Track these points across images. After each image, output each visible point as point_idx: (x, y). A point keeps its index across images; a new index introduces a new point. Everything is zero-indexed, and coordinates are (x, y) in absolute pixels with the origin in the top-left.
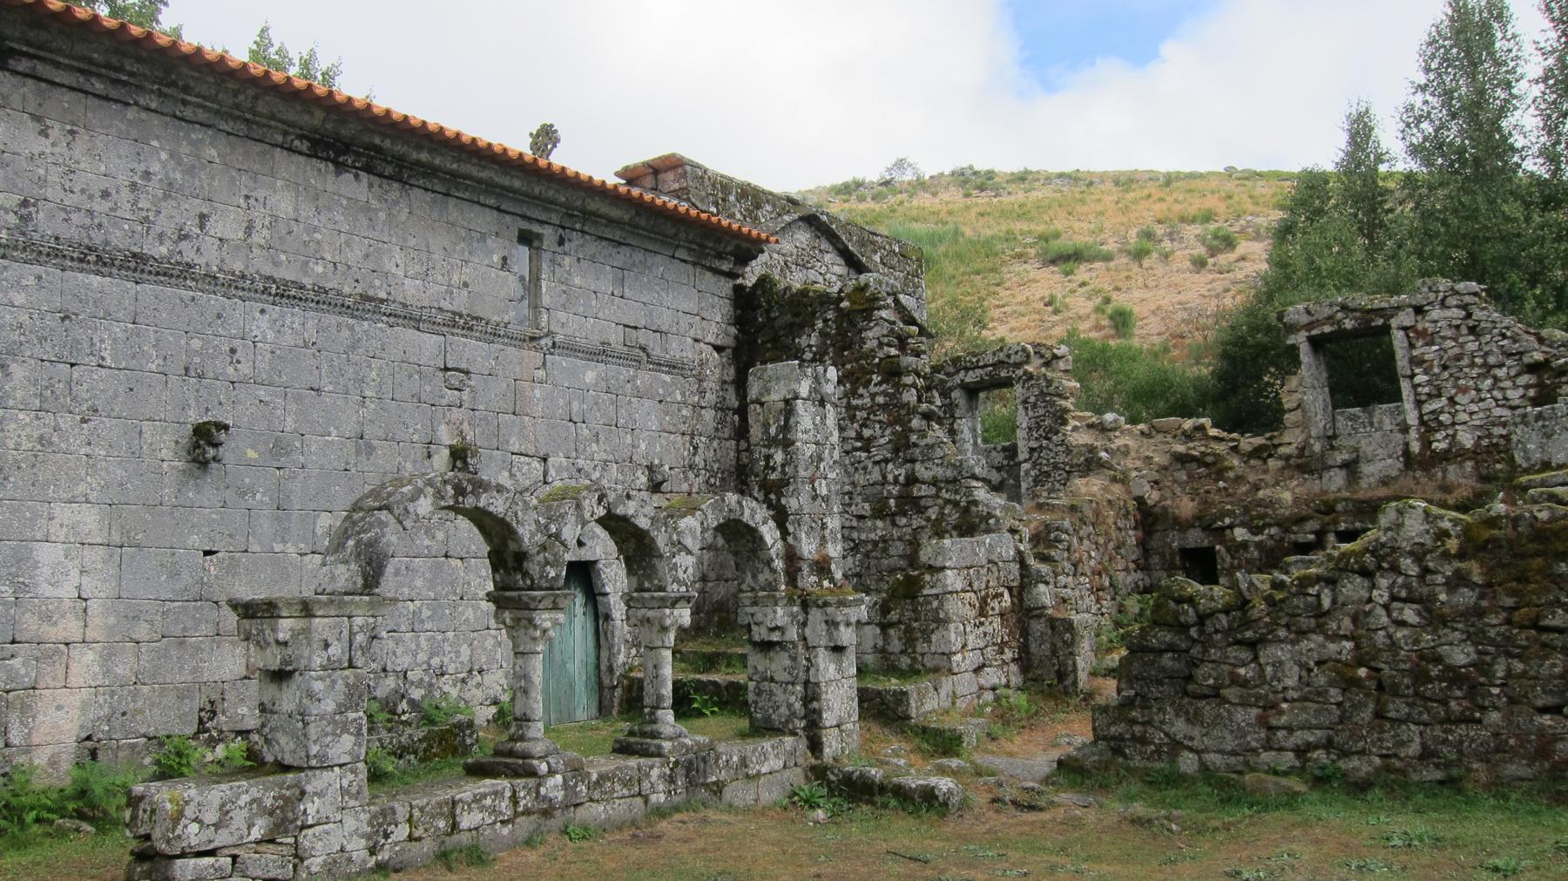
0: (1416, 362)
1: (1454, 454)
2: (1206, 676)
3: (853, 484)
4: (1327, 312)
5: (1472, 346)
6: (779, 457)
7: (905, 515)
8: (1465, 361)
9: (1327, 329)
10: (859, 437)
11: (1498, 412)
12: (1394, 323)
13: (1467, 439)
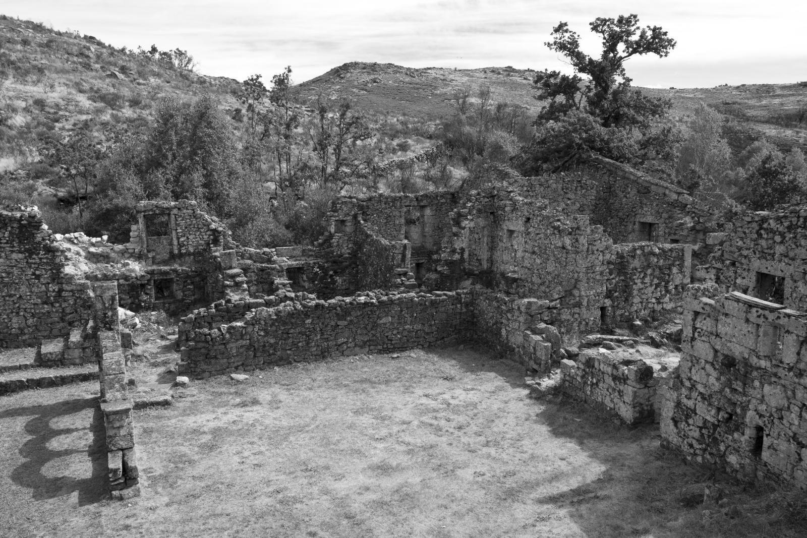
2: (213, 353)
3: (31, 292)
5: (194, 222)
6: (110, 314)
7: (58, 302)
8: (192, 226)
9: (151, 213)
10: (34, 274)
11: (200, 242)
12: (172, 213)
13: (191, 250)
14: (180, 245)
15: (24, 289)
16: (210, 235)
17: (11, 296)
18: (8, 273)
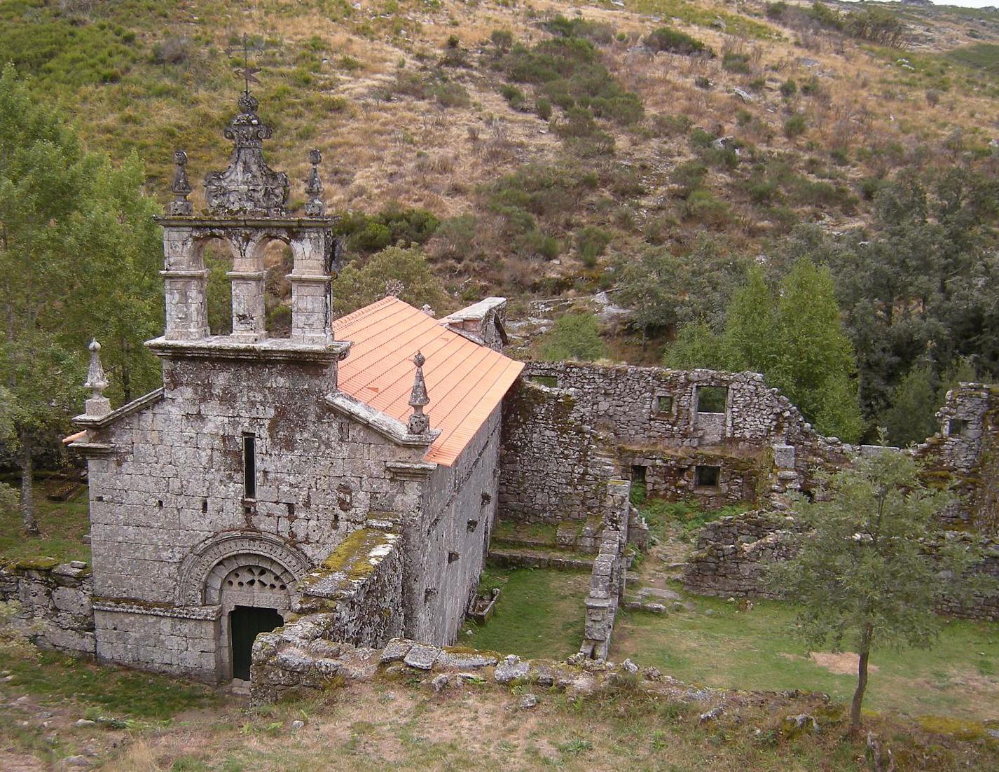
0: (735, 402)
1: (743, 439)
2: (722, 571)
4: (705, 378)
5: (755, 401)
6: (618, 513)
10: (562, 453)
13: (748, 435)
14: (735, 427)
15: (551, 466)
16: (773, 420)
17: (539, 471)
18: (540, 449)
